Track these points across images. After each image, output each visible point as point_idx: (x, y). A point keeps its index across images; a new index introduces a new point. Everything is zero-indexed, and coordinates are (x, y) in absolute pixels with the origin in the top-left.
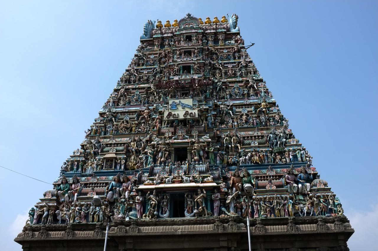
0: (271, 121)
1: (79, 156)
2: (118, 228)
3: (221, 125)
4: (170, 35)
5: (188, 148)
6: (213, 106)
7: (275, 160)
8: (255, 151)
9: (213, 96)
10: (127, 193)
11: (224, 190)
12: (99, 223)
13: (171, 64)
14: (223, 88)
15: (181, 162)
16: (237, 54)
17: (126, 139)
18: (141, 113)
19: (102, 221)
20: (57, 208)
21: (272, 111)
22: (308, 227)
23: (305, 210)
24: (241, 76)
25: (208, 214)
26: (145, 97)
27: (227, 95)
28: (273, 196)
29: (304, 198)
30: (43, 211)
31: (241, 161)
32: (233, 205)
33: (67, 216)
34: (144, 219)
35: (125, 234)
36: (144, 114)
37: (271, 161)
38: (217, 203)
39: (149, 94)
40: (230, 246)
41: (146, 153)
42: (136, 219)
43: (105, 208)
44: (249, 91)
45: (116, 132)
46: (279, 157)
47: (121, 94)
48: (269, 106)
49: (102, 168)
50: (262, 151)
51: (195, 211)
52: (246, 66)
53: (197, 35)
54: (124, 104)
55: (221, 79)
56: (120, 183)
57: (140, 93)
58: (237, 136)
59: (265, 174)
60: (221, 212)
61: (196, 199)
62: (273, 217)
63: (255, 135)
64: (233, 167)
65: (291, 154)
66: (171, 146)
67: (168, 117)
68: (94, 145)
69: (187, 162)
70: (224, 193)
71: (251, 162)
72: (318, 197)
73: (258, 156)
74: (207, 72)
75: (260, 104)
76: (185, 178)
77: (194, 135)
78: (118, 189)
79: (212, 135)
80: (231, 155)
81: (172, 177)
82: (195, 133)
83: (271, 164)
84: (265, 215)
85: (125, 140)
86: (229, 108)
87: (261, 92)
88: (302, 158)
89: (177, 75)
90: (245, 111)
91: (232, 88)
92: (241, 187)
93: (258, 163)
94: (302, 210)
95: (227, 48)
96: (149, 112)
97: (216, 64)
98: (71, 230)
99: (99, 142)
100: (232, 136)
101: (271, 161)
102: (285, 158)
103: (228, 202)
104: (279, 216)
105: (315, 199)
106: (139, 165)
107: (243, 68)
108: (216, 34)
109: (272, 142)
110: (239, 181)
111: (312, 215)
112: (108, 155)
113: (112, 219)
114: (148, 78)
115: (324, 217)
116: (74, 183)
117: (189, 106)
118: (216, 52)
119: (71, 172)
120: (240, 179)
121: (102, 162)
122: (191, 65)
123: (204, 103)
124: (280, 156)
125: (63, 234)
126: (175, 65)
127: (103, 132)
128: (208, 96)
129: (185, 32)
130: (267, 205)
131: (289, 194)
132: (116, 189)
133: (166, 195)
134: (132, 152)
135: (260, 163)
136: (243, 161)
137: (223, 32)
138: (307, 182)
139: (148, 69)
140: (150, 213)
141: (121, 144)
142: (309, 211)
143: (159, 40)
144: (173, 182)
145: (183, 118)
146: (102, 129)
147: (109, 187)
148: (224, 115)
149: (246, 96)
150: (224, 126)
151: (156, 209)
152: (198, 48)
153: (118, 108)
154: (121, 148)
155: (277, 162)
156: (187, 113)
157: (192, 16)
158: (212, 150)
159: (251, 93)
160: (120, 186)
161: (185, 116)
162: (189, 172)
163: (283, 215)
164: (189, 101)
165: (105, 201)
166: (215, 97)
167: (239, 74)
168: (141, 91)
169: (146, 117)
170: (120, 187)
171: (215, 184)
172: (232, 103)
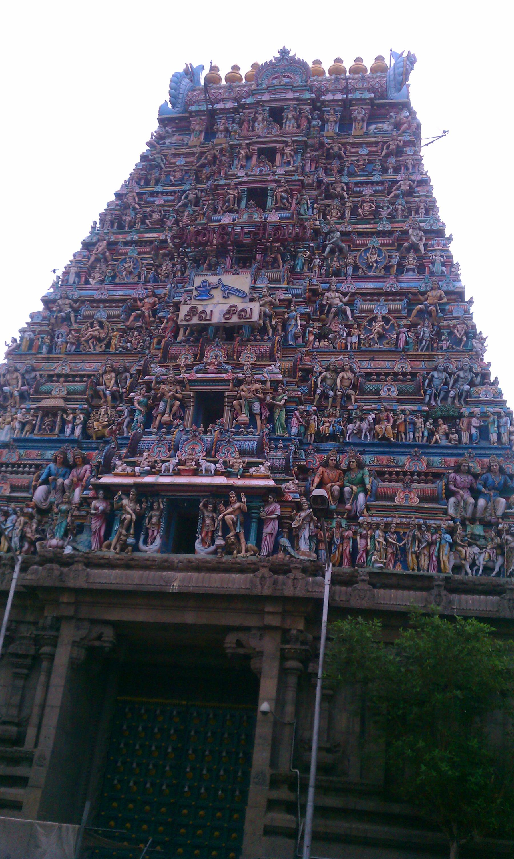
0: (443, 337)
3: (319, 342)
4: (230, 105)
6: (305, 293)
7: (431, 434)
8: (387, 410)
9: (312, 268)
10: (77, 490)
12: (10, 554)
13: (221, 182)
14: (341, 250)
15: (206, 427)
17: (93, 366)
18: (135, 304)
19: (16, 551)
24: (393, 217)
25: (247, 551)
26: (151, 264)
29: (485, 532)
31: (349, 432)
35: (58, 584)
37: (423, 437)
39: (160, 257)
40: (288, 628)
41: (131, 401)
42: (87, 551)
43: (25, 523)
44: (402, 258)
45: (74, 347)
46: (444, 427)
47: (96, 254)
48: (445, 300)
49: (32, 432)
50: (403, 411)
51: (220, 542)
52: (410, 193)
53: (298, 105)
54: (100, 280)
55: (339, 224)
57: (139, 254)
58: (351, 370)
59: (403, 466)
60: (276, 548)
61: (221, 515)
62: (399, 569)
63: (396, 370)
64: (330, 445)
65: (473, 424)
66: (188, 387)
67: (188, 318)
69: (217, 427)
70: (293, 504)
73: (392, 422)
74: (307, 204)
75: (423, 293)
76: (204, 464)
80: (329, 416)
81: (177, 461)
84: (382, 563)
86: (345, 300)
87: (433, 263)
89: (231, 211)
91: (363, 249)
92: (336, 493)
93: (388, 439)
95: (369, 144)
96: (155, 302)
100: (339, 370)
101: (423, 437)
102: (458, 432)
104: (416, 568)
106: (114, 427)
107: (401, 196)
108: (347, 104)
109: (434, 390)
110: (337, 479)
111: (498, 574)
112: (46, 400)
117: (239, 291)
120: (340, 475)
121: (33, 416)
122: (270, 186)
123: (283, 285)
124: (449, 426)
126: (229, 185)
127: (44, 346)
129: (268, 98)
130: (390, 540)
131: (447, 520)
132: (55, 480)
133: (159, 502)
134: (105, 396)
135: (392, 439)
136: (354, 431)
137: (365, 99)
139: (167, 193)
140: (118, 541)
141: (82, 376)
143: (203, 118)
144: (178, 473)
147: (42, 474)
148: (331, 316)
149: (394, 270)
150: (326, 343)
151: (132, 531)
152: (293, 142)
153: (86, 290)
154: (79, 386)
155: (437, 440)
156: (232, 311)
157: (291, 54)
158: (283, 401)
159: (409, 264)
160: (67, 474)
163: (426, 566)
166: (316, 269)
167: (384, 213)
168: (142, 249)
170: (66, 477)
171: (271, 483)
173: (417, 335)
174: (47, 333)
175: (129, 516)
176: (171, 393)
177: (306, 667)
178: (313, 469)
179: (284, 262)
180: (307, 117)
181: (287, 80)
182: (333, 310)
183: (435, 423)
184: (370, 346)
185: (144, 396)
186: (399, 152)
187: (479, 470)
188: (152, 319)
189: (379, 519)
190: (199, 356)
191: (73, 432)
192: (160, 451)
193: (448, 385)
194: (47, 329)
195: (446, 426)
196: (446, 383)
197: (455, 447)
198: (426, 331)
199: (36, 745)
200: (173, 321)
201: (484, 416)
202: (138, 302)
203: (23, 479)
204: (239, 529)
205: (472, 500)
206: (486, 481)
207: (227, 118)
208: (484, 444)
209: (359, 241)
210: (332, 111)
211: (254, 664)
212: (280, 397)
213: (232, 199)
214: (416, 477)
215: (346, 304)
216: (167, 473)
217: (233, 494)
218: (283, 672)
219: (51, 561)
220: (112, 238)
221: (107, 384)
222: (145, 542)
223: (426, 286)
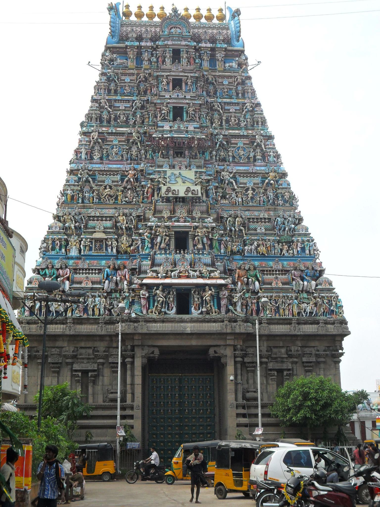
0: (280, 199)
1: (59, 233)
5: (190, 233)
7: (281, 250)
8: (262, 240)
14: (223, 144)
15: (184, 251)
16: (240, 88)
21: (282, 185)
22: (310, 328)
23: (308, 310)
25: (215, 312)
26: (127, 149)
28: (279, 294)
32: (240, 304)
34: (150, 315)
35: (134, 332)
36: (128, 175)
37: (278, 252)
38: (224, 301)
50: (269, 240)
51: (204, 309)
57: (119, 141)
58: (241, 217)
59: (272, 267)
60: (228, 311)
61: (204, 298)
62: (277, 317)
63: (261, 217)
64: (237, 257)
67: (167, 193)
71: (257, 252)
72: (323, 297)
77: (197, 217)
79: (215, 216)
80: (236, 242)
81: (178, 271)
82: (197, 214)
85: (111, 212)
86: (231, 176)
87: (270, 156)
88: (310, 251)
90: (250, 182)
92: (246, 282)
93: (264, 255)
94: (305, 309)
95: (228, 77)
98: (73, 325)
101: (278, 252)
102: (293, 249)
103: (235, 300)
105: (319, 300)
108: (213, 49)
113: (113, 312)
114: (128, 116)
115: (325, 318)
116: (61, 268)
118: (214, 81)
119: (53, 253)
121: (90, 242)
122: (185, 106)
125: (63, 328)
127: (80, 199)
128: (207, 159)
132: (112, 277)
134: (122, 229)
138: (313, 280)
139: (124, 100)
142: (312, 311)
144: (179, 277)
145: (184, 195)
146: (79, 194)
148: (226, 185)
149: (252, 160)
151: (164, 305)
152: (191, 76)
154: (109, 224)
156: (188, 190)
158: (217, 237)
161: (186, 193)
164: (190, 174)
165: (104, 292)
166: (214, 157)
167: (243, 124)
169: (132, 180)
172: (236, 169)
173: (268, 198)
174: (80, 191)
176: (164, 233)
177: (243, 359)
178: (233, 270)
179: (199, 154)
180: (193, 58)
182: (227, 182)
183: (283, 246)
184: (248, 204)
185: (149, 233)
186: (243, 83)
187: (303, 268)
188: (136, 184)
189: (267, 294)
190: (173, 211)
191: (112, 250)
192: (167, 265)
193: (285, 225)
195: (286, 246)
196: (284, 224)
197: (293, 257)
198: (271, 195)
199: (133, 400)
200: (151, 188)
201: (303, 242)
202: (126, 173)
203: (96, 277)
204: (212, 304)
205: (301, 283)
206: (307, 273)
207: (148, 52)
208: (303, 255)
209: (233, 141)
210: (205, 54)
211: (223, 360)
212: (215, 235)
213: (166, 114)
214: (277, 272)
215: (231, 178)
216: (175, 277)
217: (207, 288)
218: (236, 362)
219: (127, 321)
220: (101, 131)
222: (168, 309)
223: (269, 170)
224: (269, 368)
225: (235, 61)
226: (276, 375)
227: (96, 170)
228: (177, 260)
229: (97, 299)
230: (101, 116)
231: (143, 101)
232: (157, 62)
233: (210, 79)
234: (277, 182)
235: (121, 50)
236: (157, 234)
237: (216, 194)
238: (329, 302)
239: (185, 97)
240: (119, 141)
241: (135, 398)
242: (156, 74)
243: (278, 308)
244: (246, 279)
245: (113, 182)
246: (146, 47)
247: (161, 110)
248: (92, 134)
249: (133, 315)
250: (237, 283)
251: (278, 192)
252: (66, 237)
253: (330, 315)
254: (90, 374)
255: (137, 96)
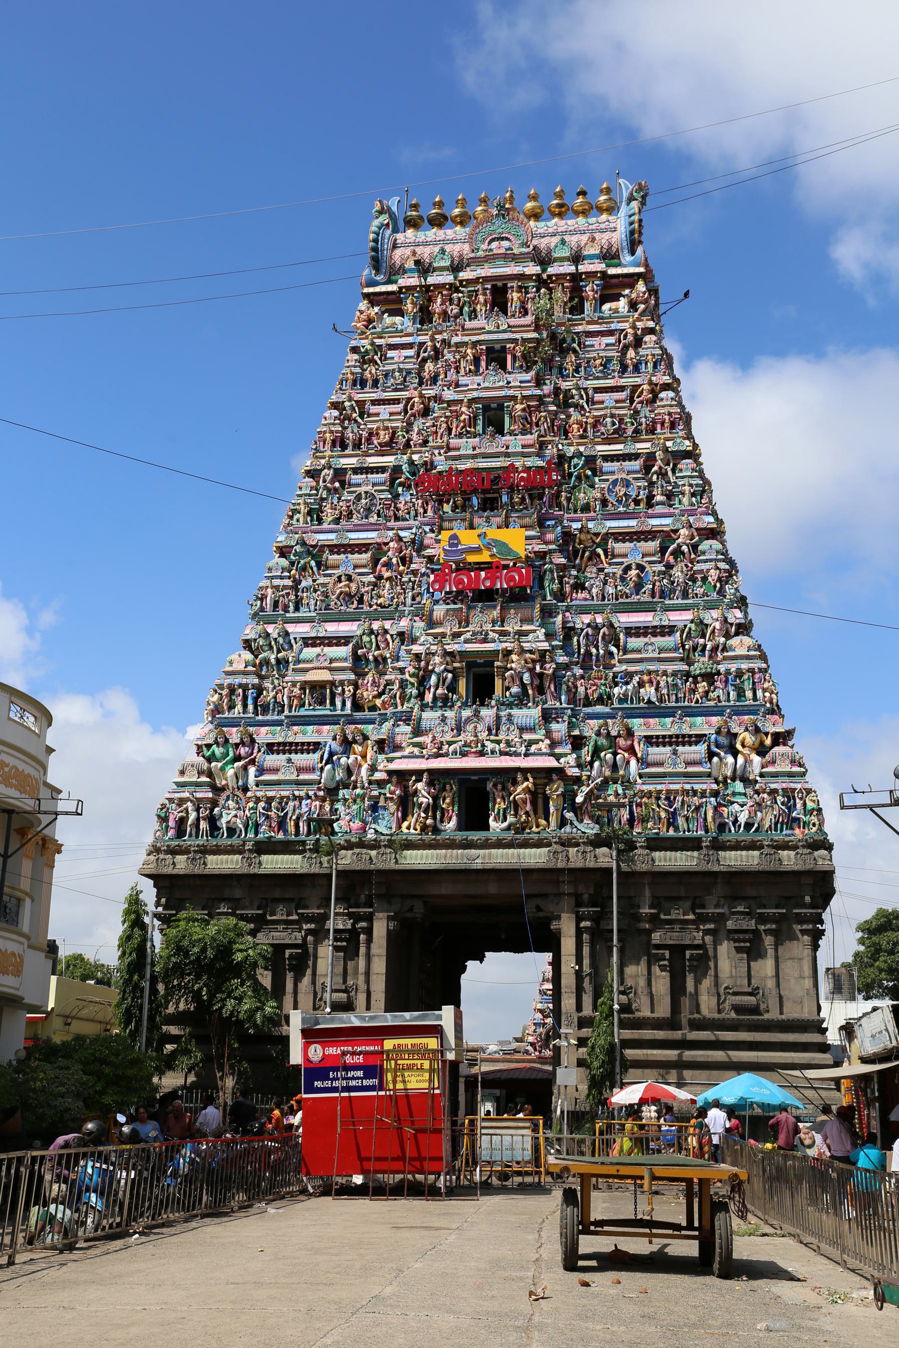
1: (245, 673)
2: (353, 854)
3: (577, 592)
8: (649, 673)
11: (574, 772)
20: (214, 803)
21: (704, 553)
23: (743, 818)
26: (387, 499)
27: (596, 500)
30: (187, 809)
33: (238, 821)
36: (389, 550)
50: (665, 673)
56: (347, 745)
58: (611, 625)
60: (563, 823)
62: (671, 832)
68: (275, 639)
75: (676, 531)
76: (490, 746)
78: (343, 760)
83: (682, 704)
86: (598, 541)
87: (683, 494)
92: (611, 762)
93: (654, 703)
94: (736, 817)
97: (574, 392)
99: (287, 634)
100: (600, 626)
105: (765, 796)
108: (576, 278)
111: (757, 830)
114: (394, 433)
118: (575, 345)
132: (339, 759)
134: (367, 660)
138: (758, 754)
142: (750, 821)
144: (464, 754)
146: (288, 594)
150: (583, 595)
158: (551, 671)
162: (497, 731)
165: (319, 789)
169: (394, 561)
174: (291, 587)
175: (425, 800)
181: (505, 244)
182: (587, 554)
183: (695, 682)
185: (415, 668)
191: (344, 704)
192: (443, 731)
194: (288, 582)
195: (705, 683)
196: (703, 636)
204: (528, 807)
207: (442, 295)
218: (579, 932)
221: (368, 646)
224: (653, 942)
225: (624, 296)
226: (667, 956)
227: (325, 546)
228: (463, 719)
229: (304, 802)
230: (343, 434)
231: (429, 398)
232: (461, 313)
233: (569, 340)
234: (695, 547)
235: (393, 297)
236: (430, 668)
237: (561, 583)
238: (789, 801)
239: (508, 383)
240: (374, 485)
241: (373, 1002)
242: (455, 340)
243: (674, 814)
244: (609, 756)
245: (355, 567)
246: (439, 287)
247: (458, 415)
248: (323, 473)
249: (371, 835)
250: (591, 764)
251: (695, 568)
252: (256, 681)
253: (792, 829)
254: (288, 952)
255: (415, 389)
